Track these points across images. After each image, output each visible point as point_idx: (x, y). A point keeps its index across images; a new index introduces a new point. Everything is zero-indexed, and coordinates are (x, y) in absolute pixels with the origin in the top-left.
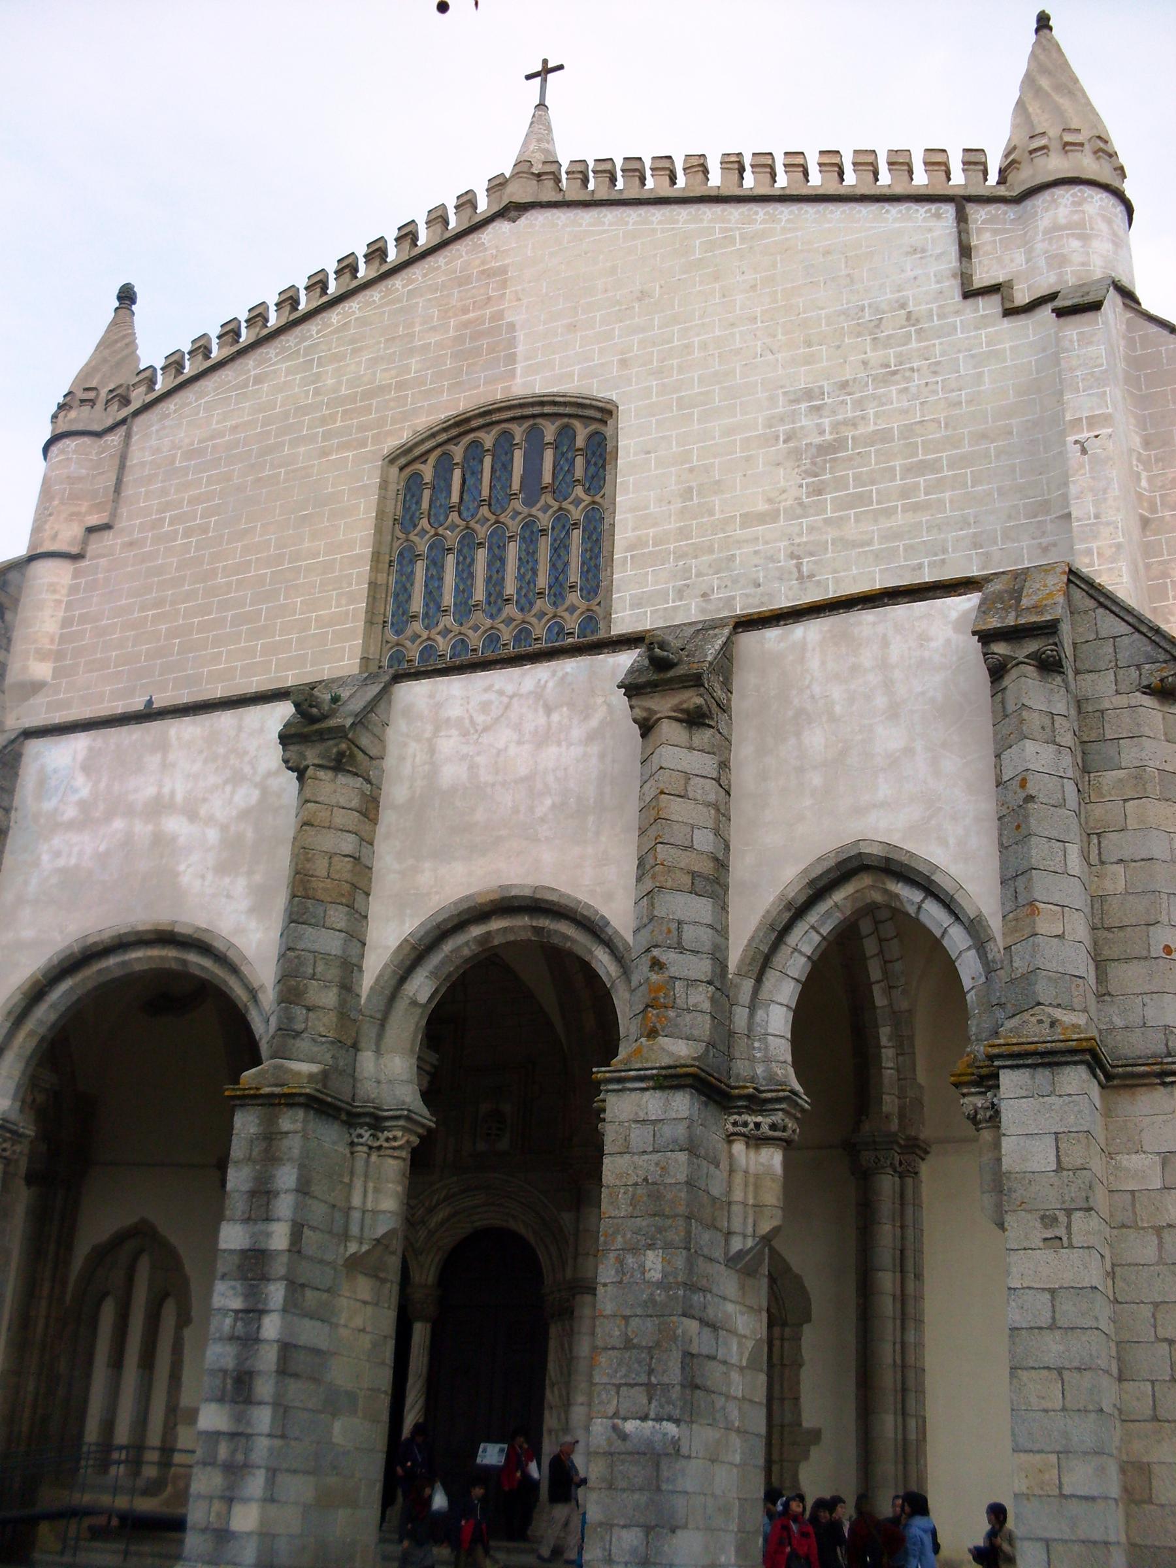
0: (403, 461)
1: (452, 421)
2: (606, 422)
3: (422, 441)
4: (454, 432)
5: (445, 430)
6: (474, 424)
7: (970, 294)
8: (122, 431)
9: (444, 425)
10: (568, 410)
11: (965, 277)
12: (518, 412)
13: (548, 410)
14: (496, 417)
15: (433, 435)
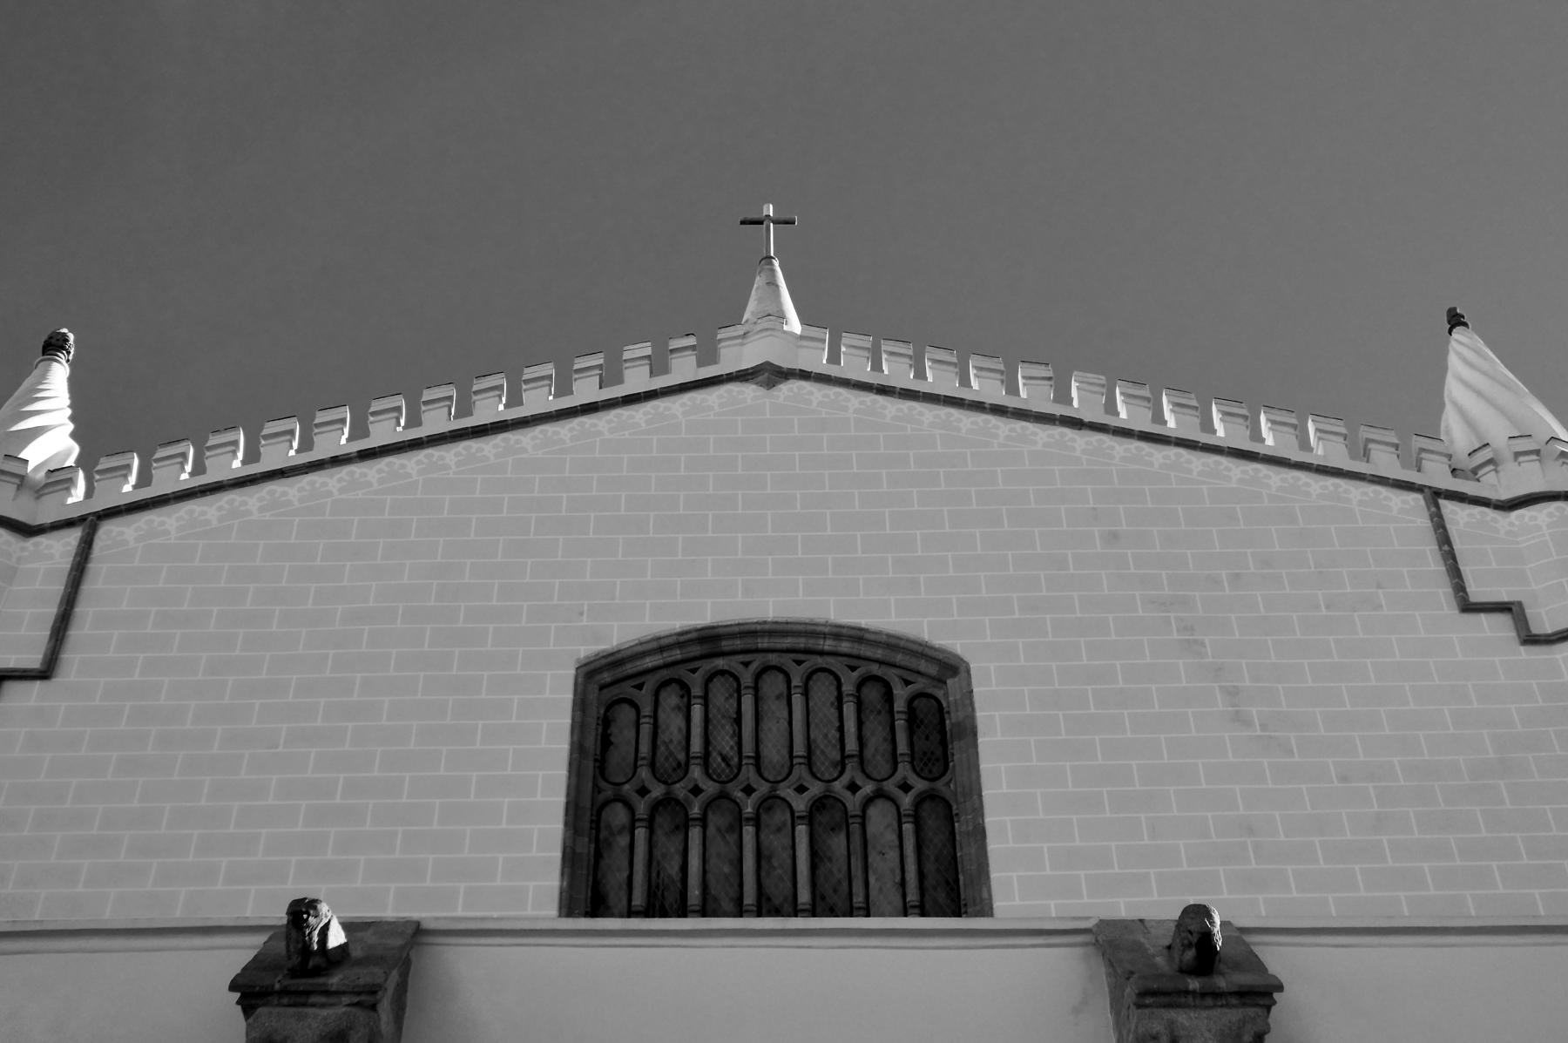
0: (607, 677)
1: (694, 635)
2: (945, 683)
3: (643, 654)
4: (696, 650)
5: (679, 645)
6: (726, 645)
7: (1468, 607)
8: (73, 537)
9: (682, 639)
10: (879, 653)
11: (1460, 588)
12: (801, 643)
13: (845, 647)
14: (764, 643)
15: (661, 649)
